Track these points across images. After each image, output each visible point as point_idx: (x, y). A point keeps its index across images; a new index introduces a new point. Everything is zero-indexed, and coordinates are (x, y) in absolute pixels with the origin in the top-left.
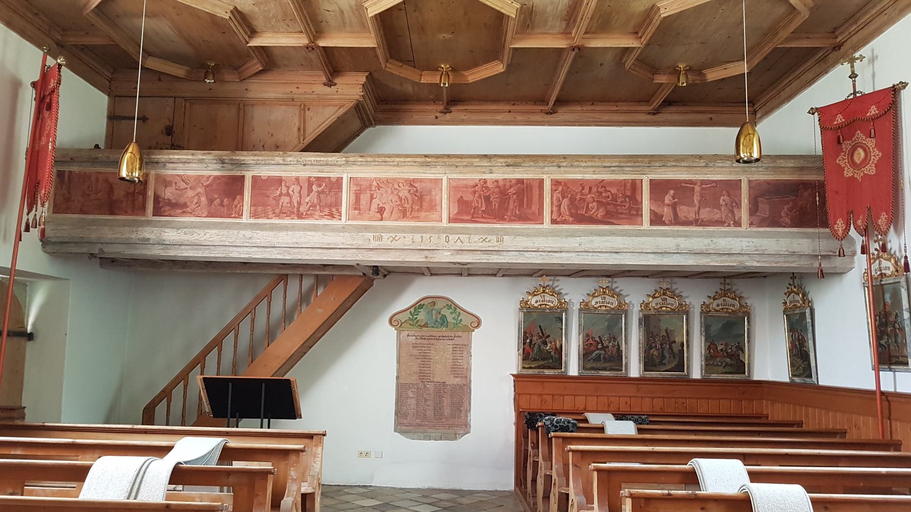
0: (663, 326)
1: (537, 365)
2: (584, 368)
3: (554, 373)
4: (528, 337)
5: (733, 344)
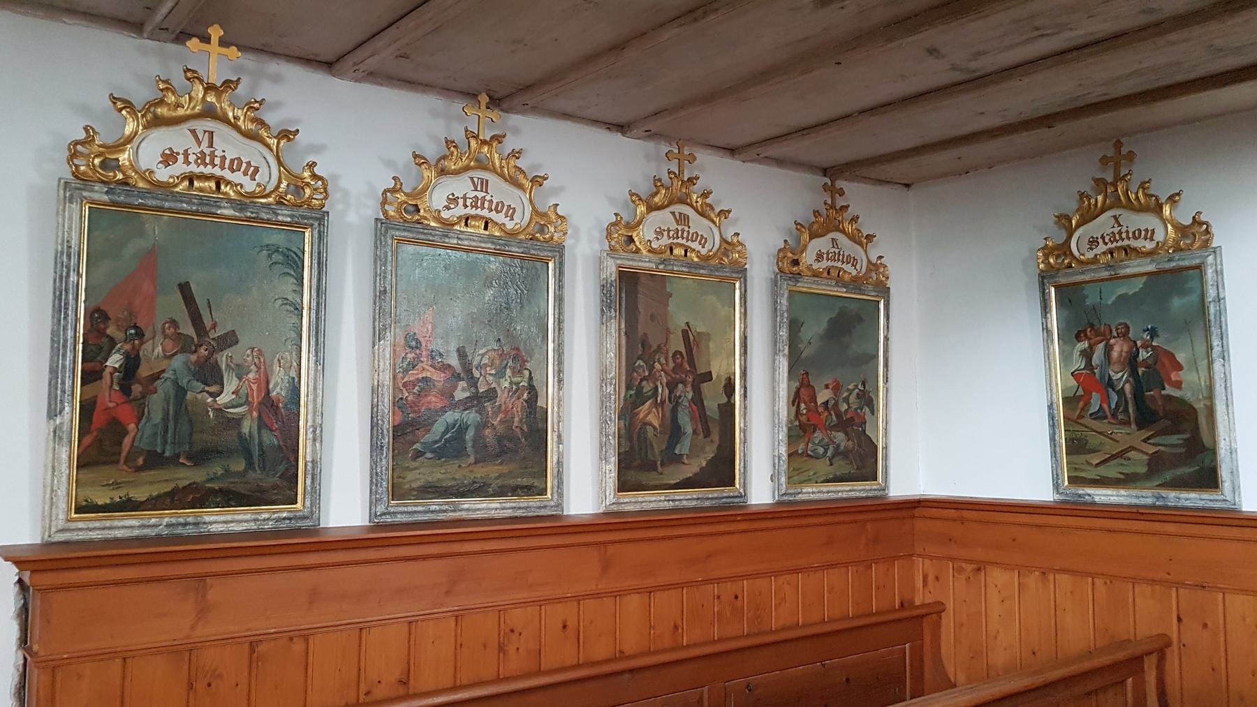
0: (679, 317)
1: (167, 488)
2: (397, 492)
3: (253, 526)
4: (112, 342)
5: (851, 387)
